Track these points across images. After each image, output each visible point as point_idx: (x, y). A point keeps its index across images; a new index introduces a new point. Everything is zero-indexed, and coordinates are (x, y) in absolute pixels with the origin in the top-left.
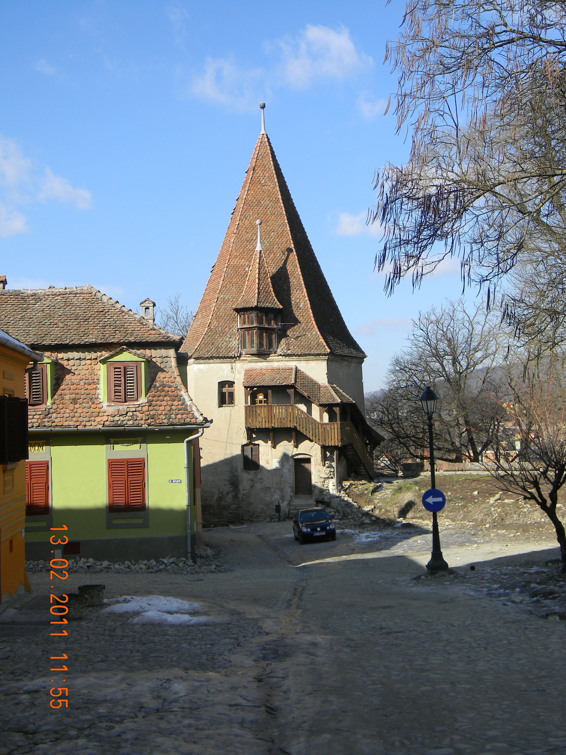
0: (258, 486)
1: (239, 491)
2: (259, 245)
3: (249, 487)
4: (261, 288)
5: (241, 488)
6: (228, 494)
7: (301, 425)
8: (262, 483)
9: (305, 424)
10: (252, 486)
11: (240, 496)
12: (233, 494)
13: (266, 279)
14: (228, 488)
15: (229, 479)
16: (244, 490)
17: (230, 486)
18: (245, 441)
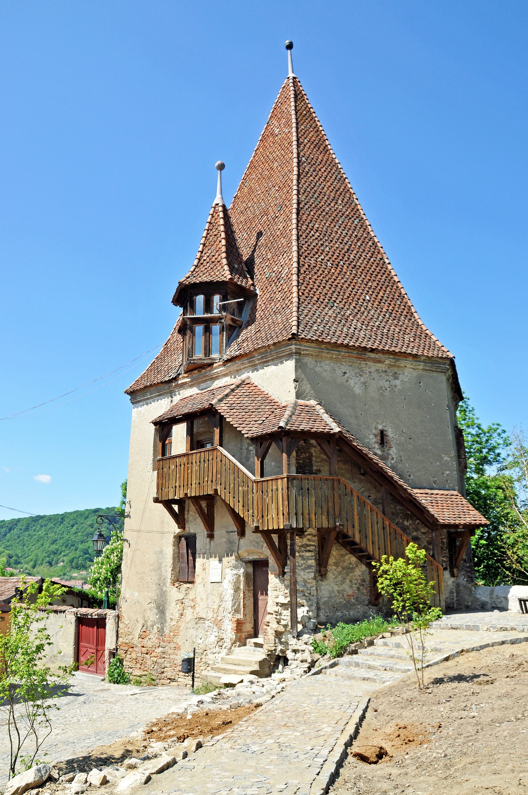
0: (189, 614)
1: (165, 620)
2: (218, 196)
3: (177, 615)
4: (205, 258)
5: (168, 615)
6: (153, 626)
7: (227, 487)
8: (193, 607)
9: (232, 486)
10: (182, 615)
11: (167, 631)
12: (159, 626)
13: (217, 242)
14: (152, 616)
15: (156, 598)
16: (171, 619)
17: (155, 611)
18: (178, 531)
